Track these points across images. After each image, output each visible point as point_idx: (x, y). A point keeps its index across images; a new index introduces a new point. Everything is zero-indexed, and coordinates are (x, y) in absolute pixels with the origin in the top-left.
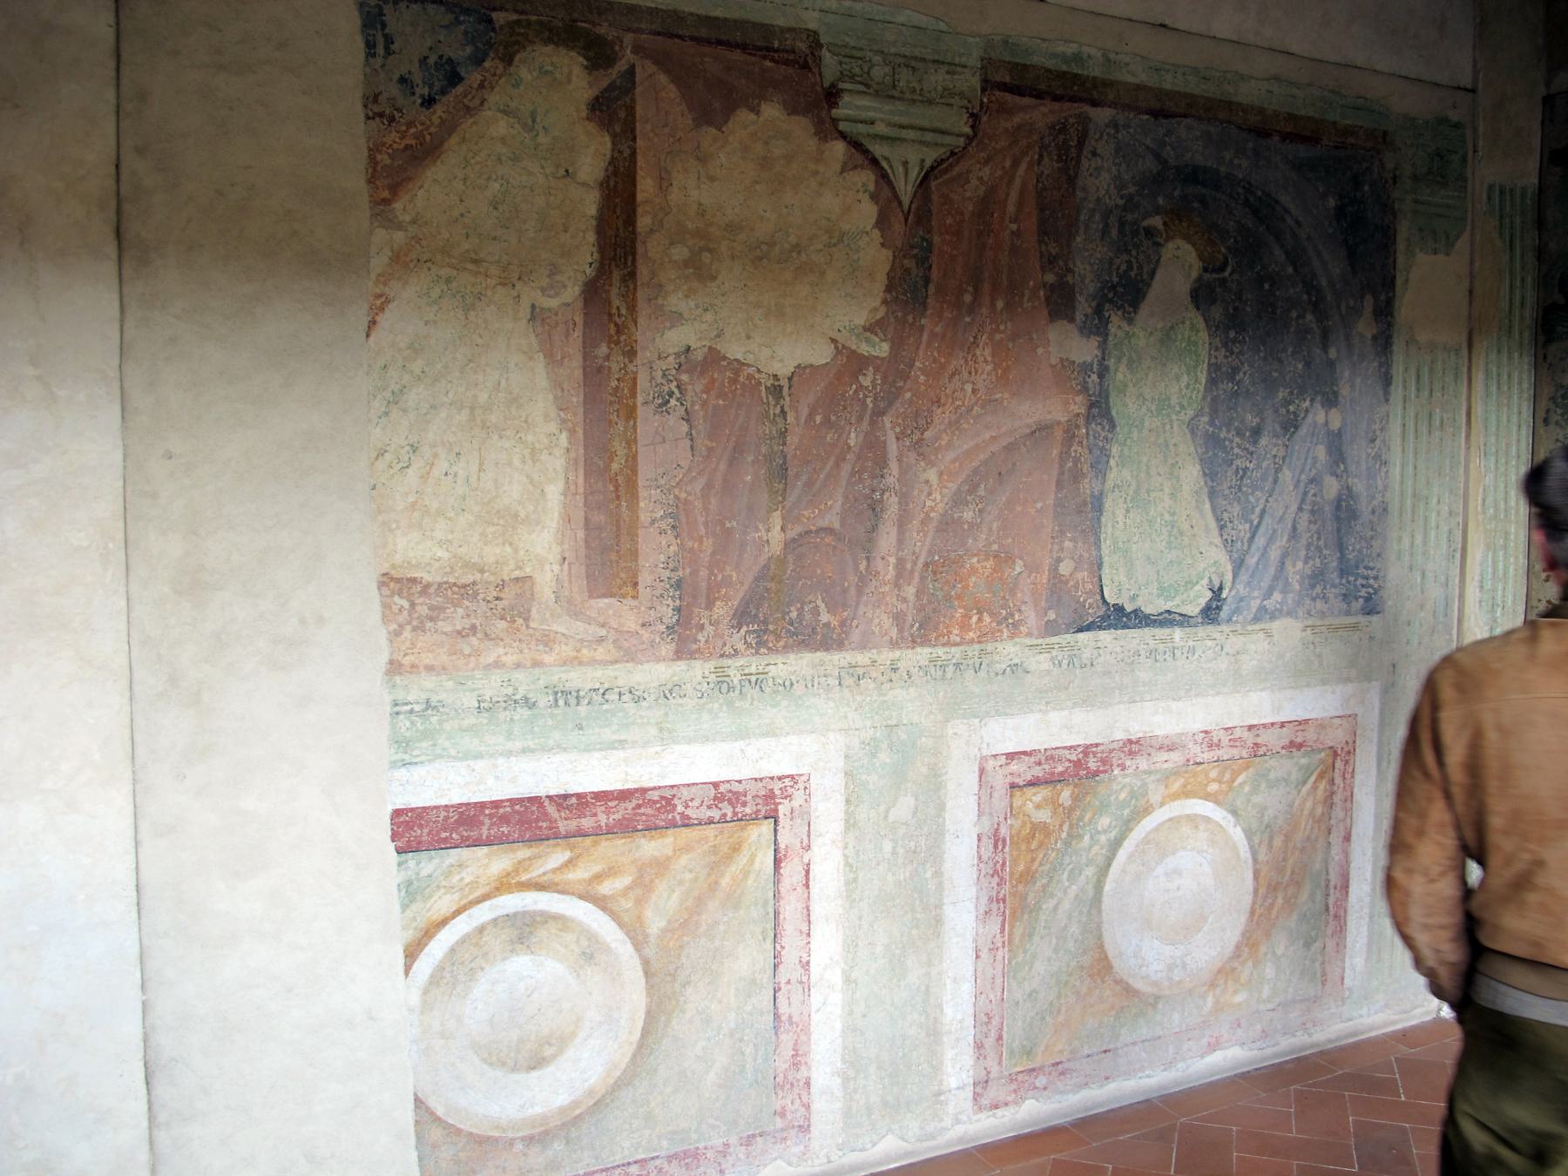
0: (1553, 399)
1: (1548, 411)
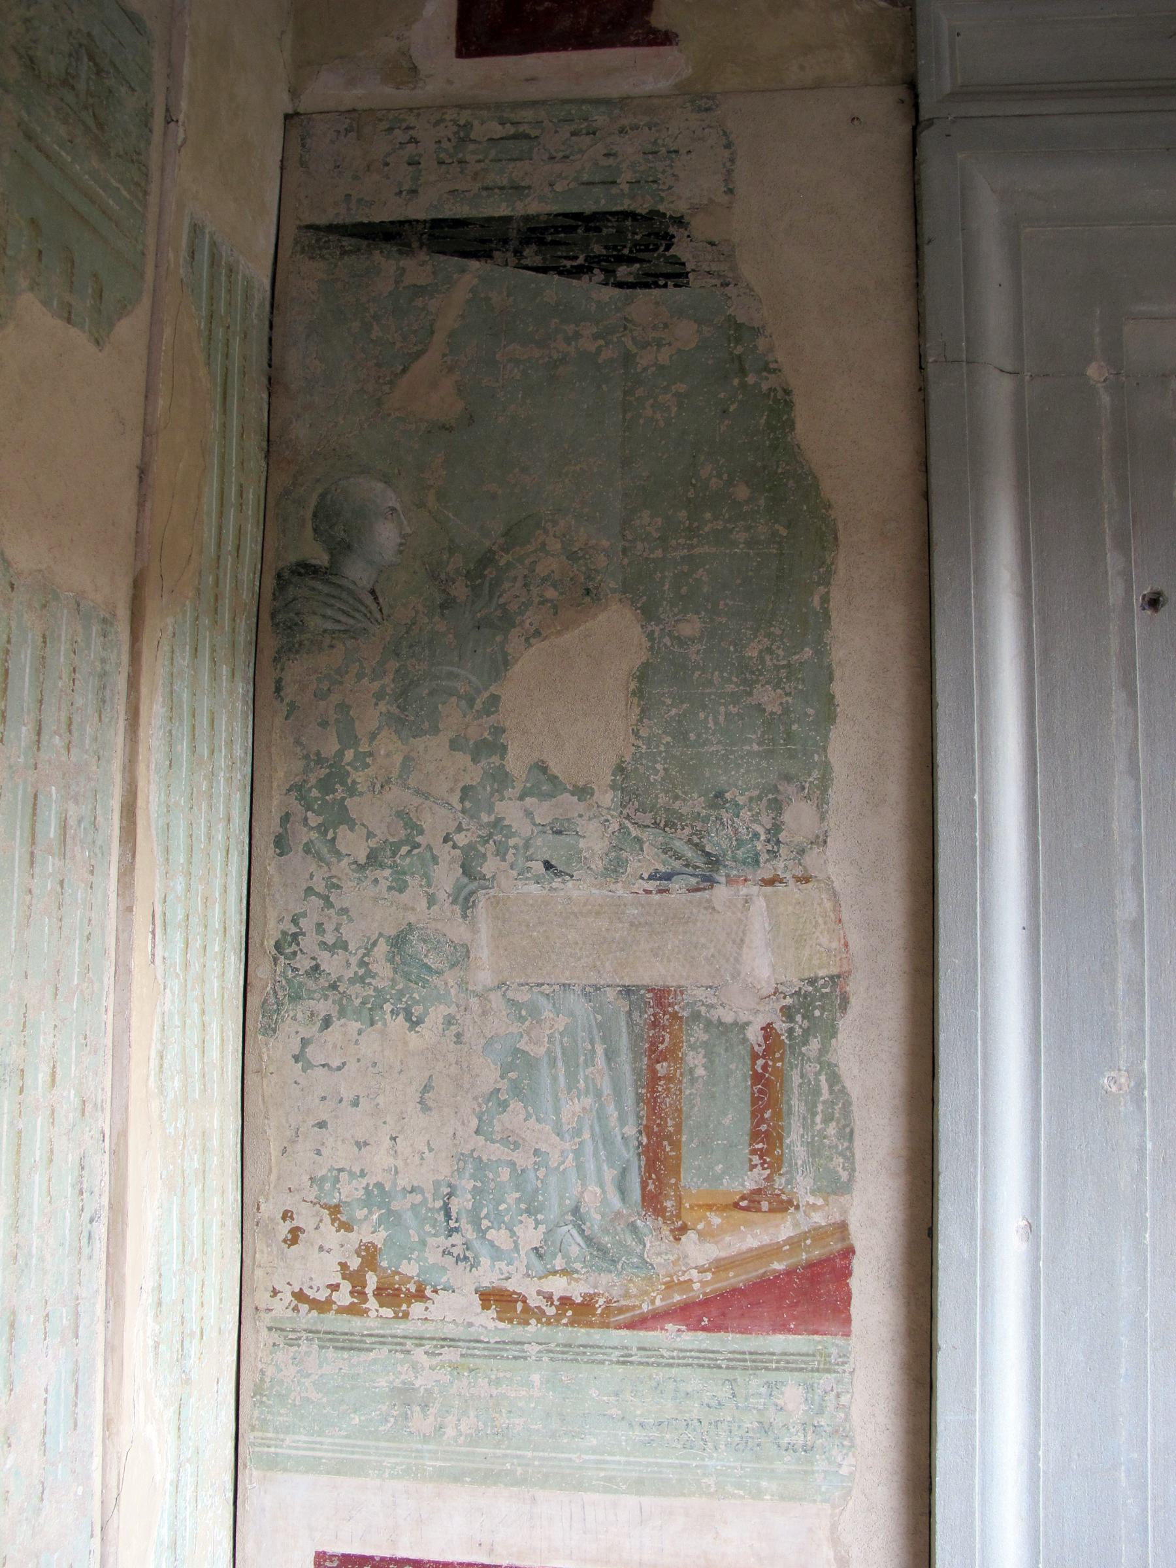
0: (298, 789)
1: (286, 819)
